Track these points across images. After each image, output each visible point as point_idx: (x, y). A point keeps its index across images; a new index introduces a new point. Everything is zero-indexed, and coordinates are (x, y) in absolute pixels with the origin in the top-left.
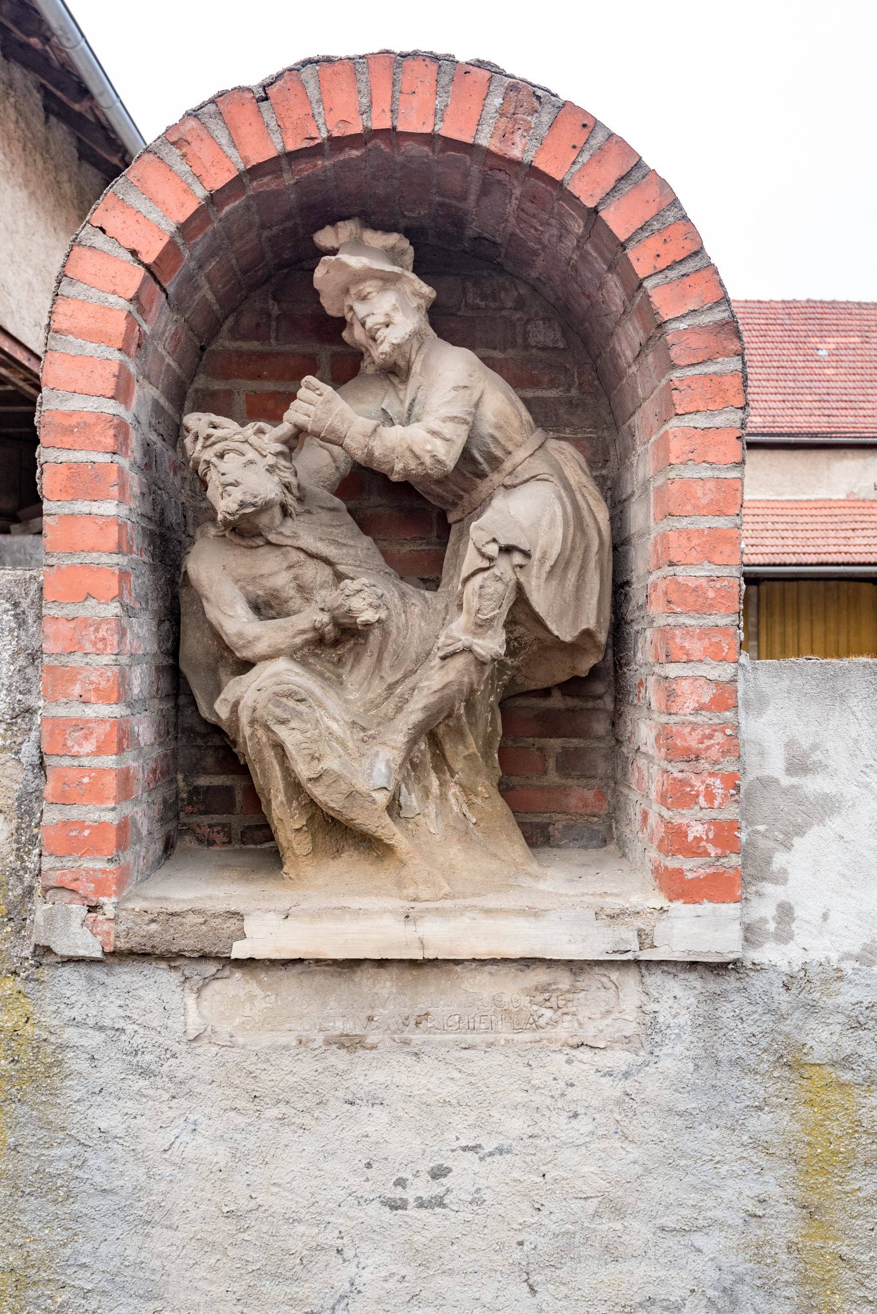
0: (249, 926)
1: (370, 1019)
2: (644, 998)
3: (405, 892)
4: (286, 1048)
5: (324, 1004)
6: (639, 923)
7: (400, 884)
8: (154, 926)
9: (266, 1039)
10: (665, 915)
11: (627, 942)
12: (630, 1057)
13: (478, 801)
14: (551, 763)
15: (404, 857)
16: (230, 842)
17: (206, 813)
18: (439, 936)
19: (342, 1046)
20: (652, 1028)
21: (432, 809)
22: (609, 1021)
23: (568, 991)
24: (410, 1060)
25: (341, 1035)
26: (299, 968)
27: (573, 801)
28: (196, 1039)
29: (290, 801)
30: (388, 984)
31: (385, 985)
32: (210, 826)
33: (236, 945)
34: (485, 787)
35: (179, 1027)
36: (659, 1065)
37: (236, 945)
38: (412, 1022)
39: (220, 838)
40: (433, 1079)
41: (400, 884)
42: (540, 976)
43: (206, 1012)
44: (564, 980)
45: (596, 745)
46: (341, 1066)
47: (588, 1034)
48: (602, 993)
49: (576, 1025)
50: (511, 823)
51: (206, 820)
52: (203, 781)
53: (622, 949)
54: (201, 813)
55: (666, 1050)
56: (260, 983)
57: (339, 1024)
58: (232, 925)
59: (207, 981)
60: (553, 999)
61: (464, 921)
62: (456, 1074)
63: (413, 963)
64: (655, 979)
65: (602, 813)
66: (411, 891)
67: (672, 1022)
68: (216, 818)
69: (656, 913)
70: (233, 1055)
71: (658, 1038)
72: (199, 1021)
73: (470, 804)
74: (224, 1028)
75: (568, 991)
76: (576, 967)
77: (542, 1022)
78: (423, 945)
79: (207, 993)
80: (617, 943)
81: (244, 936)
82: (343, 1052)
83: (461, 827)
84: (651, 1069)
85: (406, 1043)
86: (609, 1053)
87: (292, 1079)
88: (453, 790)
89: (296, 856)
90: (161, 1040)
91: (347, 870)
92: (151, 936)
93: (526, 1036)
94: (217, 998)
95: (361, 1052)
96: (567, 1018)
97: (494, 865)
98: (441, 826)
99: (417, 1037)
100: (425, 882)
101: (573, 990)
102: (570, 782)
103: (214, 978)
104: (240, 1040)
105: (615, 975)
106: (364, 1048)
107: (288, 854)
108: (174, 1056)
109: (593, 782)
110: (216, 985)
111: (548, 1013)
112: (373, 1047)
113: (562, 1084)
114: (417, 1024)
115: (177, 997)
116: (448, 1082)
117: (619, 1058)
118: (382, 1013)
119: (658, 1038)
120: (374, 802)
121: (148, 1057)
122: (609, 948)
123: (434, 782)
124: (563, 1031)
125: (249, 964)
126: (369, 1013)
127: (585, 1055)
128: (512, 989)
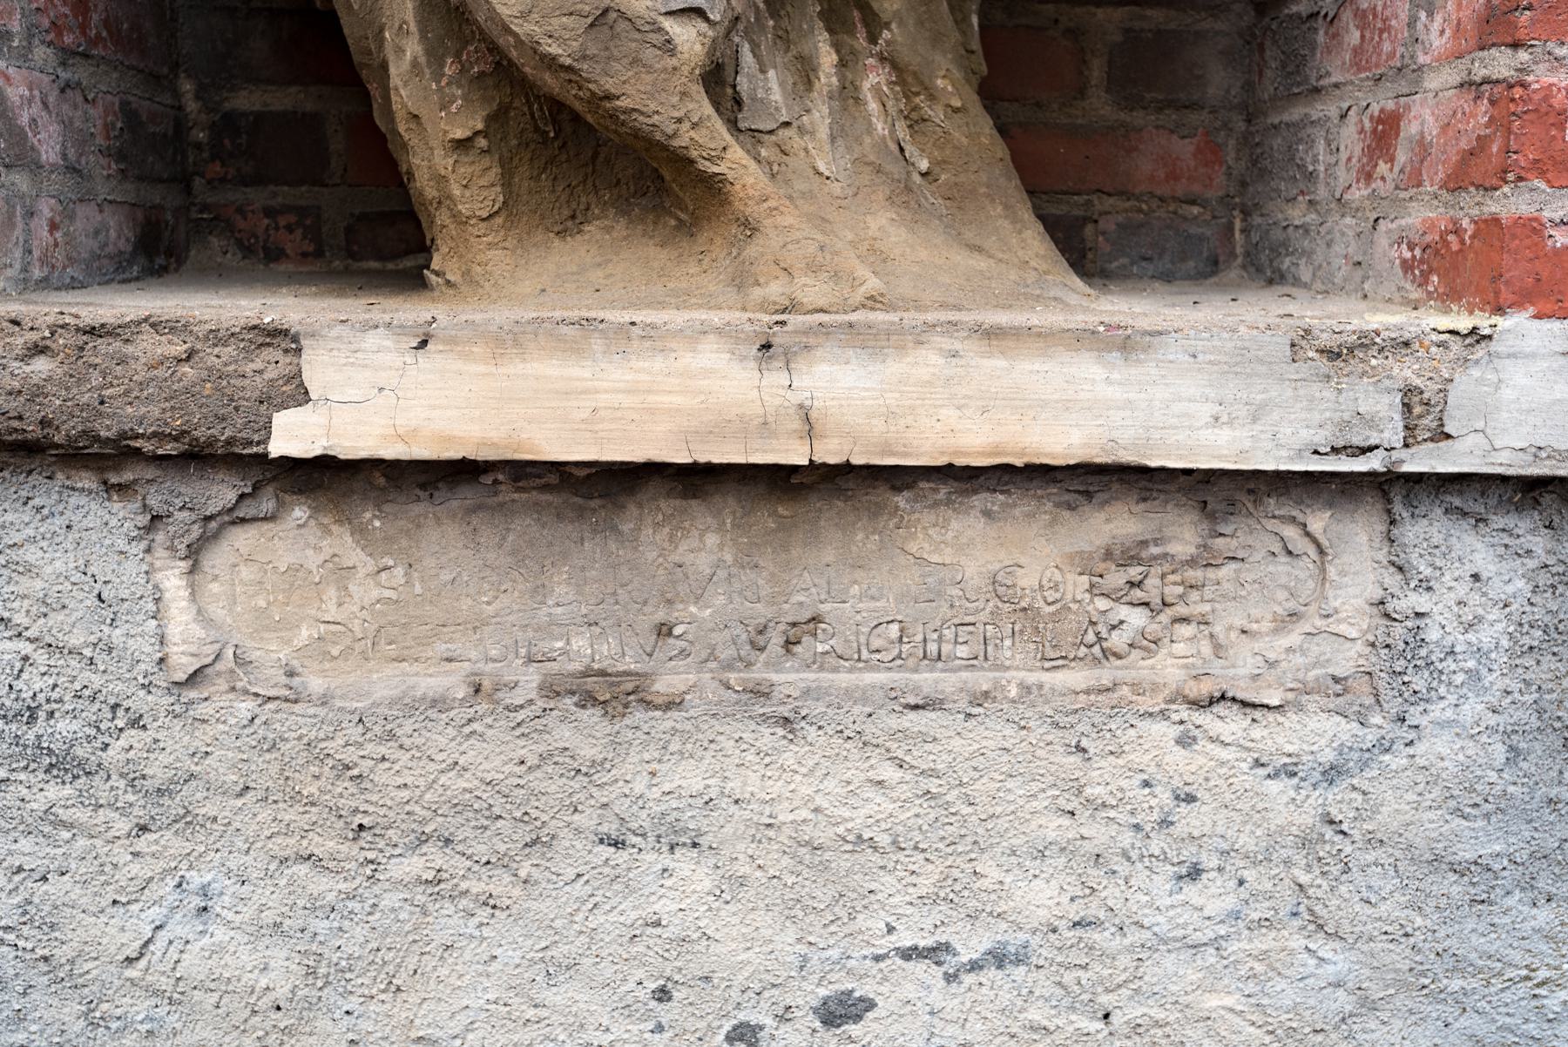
0: (318, 368)
1: (664, 631)
2: (1392, 580)
3: (757, 293)
4: (439, 703)
5: (540, 592)
6: (1406, 371)
7: (742, 280)
8: (41, 365)
9: (383, 683)
10: (1480, 352)
11: (1370, 422)
12: (1346, 729)
13: (937, 114)
14: (1097, 71)
15: (753, 210)
16: (319, 254)
17: (257, 180)
18: (862, 401)
19: (588, 699)
20: (1406, 656)
21: (820, 116)
22: (1294, 638)
23: (1192, 562)
24: (768, 737)
25: (587, 673)
26: (467, 495)
27: (1144, 167)
28: (194, 678)
29: (435, 56)
30: (712, 539)
31: (703, 544)
32: (269, 212)
33: (281, 419)
34: (950, 83)
35: (146, 648)
36: (1419, 748)
37: (281, 419)
38: (776, 640)
39: (293, 242)
40: (830, 785)
41: (742, 280)
42: (1118, 522)
43: (217, 611)
44: (1183, 534)
45: (1206, 25)
46: (588, 752)
47: (1239, 670)
48: (1282, 566)
49: (1206, 648)
50: (1012, 186)
51: (257, 197)
52: (246, 101)
53: (1357, 441)
54: (245, 181)
55: (1437, 711)
56: (360, 532)
57: (580, 643)
58: (269, 365)
59: (214, 527)
60: (1152, 582)
61: (927, 362)
62: (889, 773)
63: (778, 482)
64: (1425, 531)
65: (1212, 194)
66: (775, 290)
67: (1460, 640)
68: (285, 195)
69: (1456, 345)
70: (296, 723)
71: (1419, 682)
72: (198, 631)
73: (916, 122)
74: (271, 653)
75: (1192, 562)
76: (1219, 493)
77: (1117, 640)
78: (809, 426)
79: (218, 558)
80: (1344, 425)
81: (302, 397)
82: (591, 715)
83: (896, 169)
84: (1395, 761)
85: (760, 692)
86: (1291, 719)
87: (457, 783)
88: (874, 78)
89: (461, 221)
90: (97, 681)
91: (598, 270)
92: (37, 393)
93: (1076, 677)
94: (246, 573)
95: (639, 716)
96: (1186, 630)
97: (980, 263)
98: (846, 162)
99: (788, 678)
100: (813, 268)
101: (1206, 559)
102: (1138, 118)
103: (234, 518)
104: (315, 684)
105: (1318, 522)
106: (648, 705)
107: (442, 217)
108: (136, 723)
109: (1194, 118)
110: (242, 539)
111: (1136, 618)
112: (672, 704)
113: (1164, 797)
114: (789, 644)
115: (132, 568)
116: (870, 792)
117: (1318, 732)
118: (693, 615)
119: (1419, 682)
120: (668, 46)
121: (64, 726)
122: (1322, 438)
123: (827, 58)
124: (1168, 668)
125: (326, 479)
126: (660, 616)
127: (1231, 724)
128: (1040, 554)
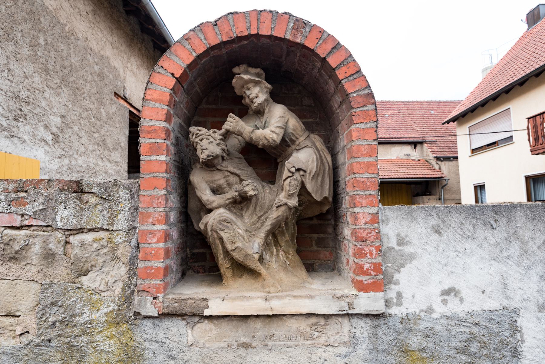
0: (210, 303)
1: (253, 337)
2: (351, 327)
3: (265, 290)
4: (223, 348)
5: (237, 331)
6: (348, 300)
7: (263, 287)
8: (176, 304)
9: (216, 345)
10: (357, 297)
11: (344, 307)
12: (346, 350)
13: (290, 256)
14: (314, 243)
15: (265, 277)
16: (205, 272)
17: (197, 262)
18: (278, 306)
19: (243, 347)
20: (354, 338)
21: (274, 260)
22: (338, 336)
23: (324, 325)
24: (268, 352)
25: (243, 343)
27: (322, 256)
28: (191, 345)
29: (225, 258)
30: (260, 324)
31: (259, 324)
32: (198, 266)
33: (206, 310)
34: (292, 251)
35: (185, 341)
36: (357, 352)
37: (206, 310)
38: (268, 338)
39: (201, 270)
40: (276, 359)
41: (263, 287)
42: (313, 320)
43: (195, 335)
44: (322, 321)
45: (329, 236)
46: (243, 355)
47: (331, 341)
48: (336, 326)
49: (327, 338)
50: (301, 264)
51: (196, 264)
52: (196, 251)
53: (343, 309)
54: (195, 262)
55: (359, 346)
56: (214, 324)
57: (242, 339)
58: (204, 303)
59: (195, 324)
60: (319, 328)
61: (286, 300)
62: (284, 357)
63: (268, 316)
64: (354, 320)
65: (332, 259)
66: (267, 290)
67: (361, 336)
68: (200, 264)
69: (354, 296)
70: (204, 351)
71: (356, 342)
72: (192, 338)
73: (287, 258)
74: (201, 341)
75: (324, 325)
76: (326, 316)
77: (315, 337)
78: (272, 309)
79: (196, 328)
80: (341, 307)
81: (208, 307)
82: (244, 349)
83: (284, 266)
84: (354, 354)
85: (266, 345)
86: (339, 348)
87: (225, 360)
88: (281, 253)
89: (227, 277)
90: (179, 346)
91: (245, 282)
92: (175, 308)
93: (309, 342)
94: (199, 330)
95: (250, 349)
96: (324, 335)
97: (296, 279)
98: (277, 265)
99: (270, 343)
100: (272, 286)
101: (325, 325)
102: (320, 249)
103: (198, 323)
104: (207, 345)
105: (340, 319)
106: (251, 348)
107: (224, 276)
108: (183, 352)
109: (328, 249)
110: (198, 325)
111: (317, 334)
112: (255, 347)
113: (323, 360)
114: (270, 338)
115: (185, 330)
116: (282, 360)
117: (343, 350)
118: (257, 335)
119: (356, 342)
120: (254, 258)
121: (174, 352)
122: (338, 309)
123: (275, 250)
124: (322, 340)
125: (210, 318)
126: (253, 334)
127: (330, 349)
128: (304, 325)
